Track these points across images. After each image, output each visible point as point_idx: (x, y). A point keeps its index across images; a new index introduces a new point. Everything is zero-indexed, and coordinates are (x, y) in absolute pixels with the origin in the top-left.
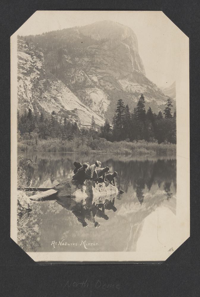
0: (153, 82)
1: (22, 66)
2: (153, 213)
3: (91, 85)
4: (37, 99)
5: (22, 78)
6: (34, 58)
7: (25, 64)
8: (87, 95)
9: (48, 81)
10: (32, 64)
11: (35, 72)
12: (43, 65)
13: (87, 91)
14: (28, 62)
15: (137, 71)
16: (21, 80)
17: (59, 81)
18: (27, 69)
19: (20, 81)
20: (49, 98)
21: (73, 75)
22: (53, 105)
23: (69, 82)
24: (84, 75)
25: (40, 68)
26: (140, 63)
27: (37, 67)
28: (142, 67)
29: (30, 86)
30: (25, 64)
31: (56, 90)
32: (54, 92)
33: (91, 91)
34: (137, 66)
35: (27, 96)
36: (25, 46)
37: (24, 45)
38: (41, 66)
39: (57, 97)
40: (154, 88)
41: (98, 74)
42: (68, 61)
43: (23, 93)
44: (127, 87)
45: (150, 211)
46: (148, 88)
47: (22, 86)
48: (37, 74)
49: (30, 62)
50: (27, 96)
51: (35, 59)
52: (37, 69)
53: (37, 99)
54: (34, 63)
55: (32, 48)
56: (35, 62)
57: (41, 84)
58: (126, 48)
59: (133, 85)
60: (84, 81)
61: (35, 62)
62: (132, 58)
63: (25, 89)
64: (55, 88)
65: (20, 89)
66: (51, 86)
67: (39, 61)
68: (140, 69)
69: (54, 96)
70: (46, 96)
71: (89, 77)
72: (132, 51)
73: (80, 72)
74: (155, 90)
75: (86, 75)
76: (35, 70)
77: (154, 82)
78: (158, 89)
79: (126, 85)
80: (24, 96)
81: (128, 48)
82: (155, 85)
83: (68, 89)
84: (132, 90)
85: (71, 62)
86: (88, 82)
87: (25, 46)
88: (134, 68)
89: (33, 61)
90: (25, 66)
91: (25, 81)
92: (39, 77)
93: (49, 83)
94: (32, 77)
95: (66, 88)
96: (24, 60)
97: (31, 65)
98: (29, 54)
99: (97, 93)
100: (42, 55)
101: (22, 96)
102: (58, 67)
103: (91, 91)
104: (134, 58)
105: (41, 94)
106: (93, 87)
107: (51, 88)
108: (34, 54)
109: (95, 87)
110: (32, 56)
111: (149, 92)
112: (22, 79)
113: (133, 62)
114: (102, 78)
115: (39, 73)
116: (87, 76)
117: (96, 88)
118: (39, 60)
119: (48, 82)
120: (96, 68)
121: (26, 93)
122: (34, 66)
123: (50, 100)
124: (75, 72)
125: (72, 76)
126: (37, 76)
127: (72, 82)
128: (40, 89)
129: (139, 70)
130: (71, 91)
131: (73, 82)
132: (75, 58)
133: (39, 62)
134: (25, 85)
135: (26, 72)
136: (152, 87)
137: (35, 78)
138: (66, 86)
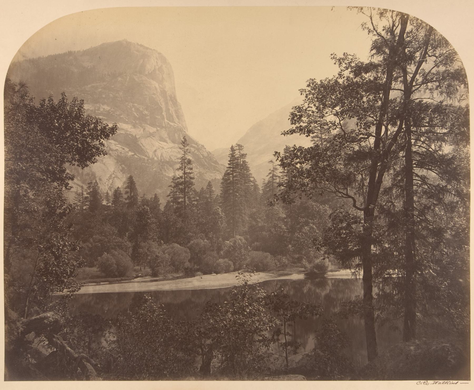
15: (172, 124)
26: (177, 112)
34: (172, 116)
40: (201, 151)
58: (153, 86)
59: (165, 147)
62: (163, 104)
68: (176, 120)
72: (164, 93)
74: (202, 155)
78: (207, 153)
79: (155, 148)
81: (155, 87)
84: (164, 155)
99: (104, 162)
104: (167, 104)
113: (164, 109)
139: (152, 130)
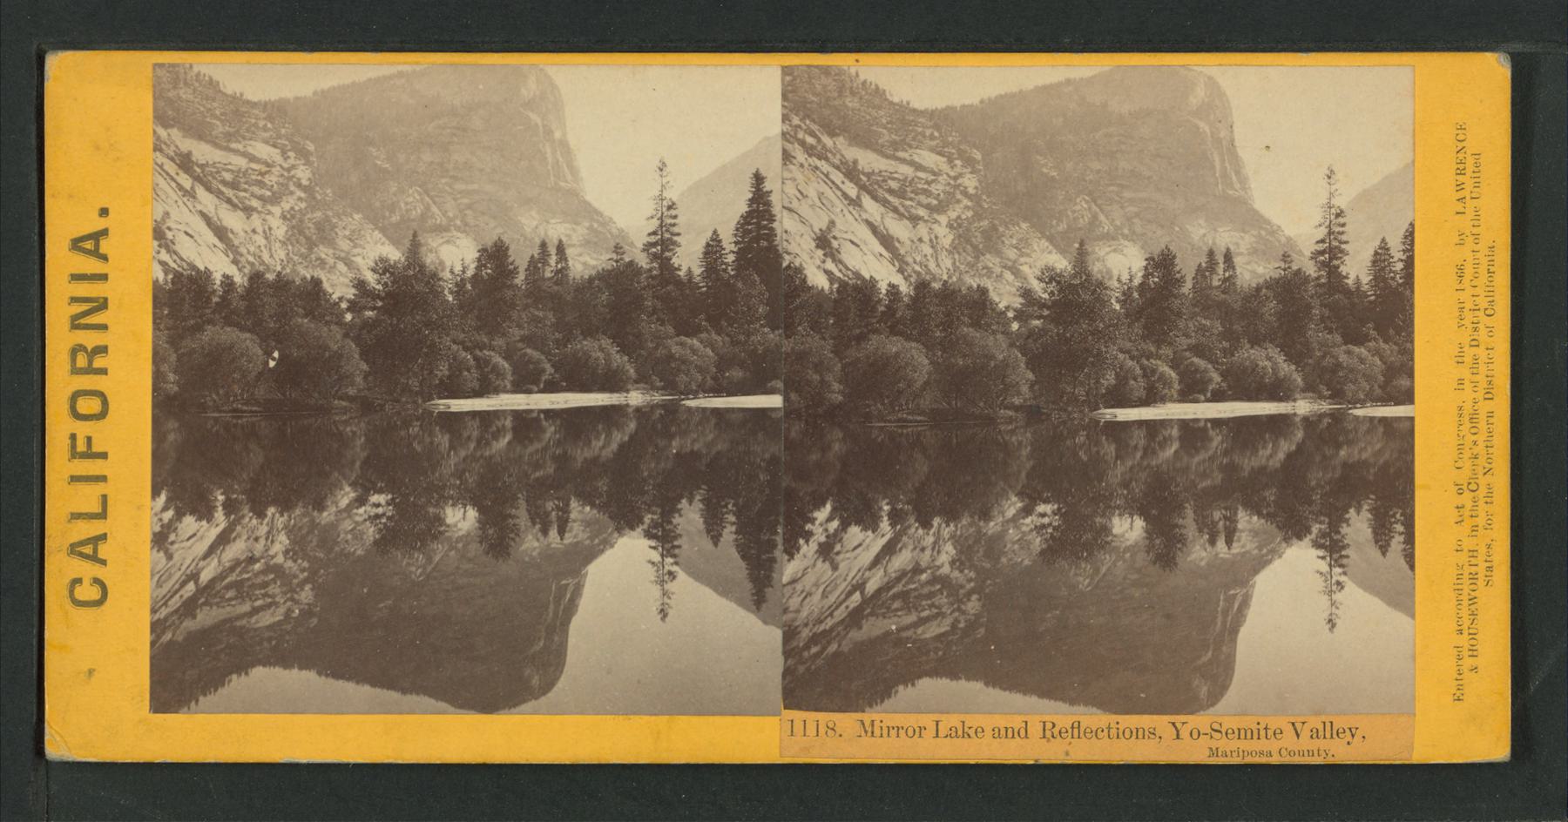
0: (606, 214)
1: (259, 178)
2: (609, 553)
3: (440, 225)
4: (301, 263)
5: (260, 209)
6: (289, 157)
7: (266, 173)
8: (431, 251)
9: (327, 216)
10: (286, 174)
11: (292, 193)
12: (314, 174)
13: (430, 240)
14: (273, 170)
16: (255, 216)
17: (356, 217)
18: (272, 186)
19: (252, 218)
20: (331, 261)
22: (342, 279)
23: (384, 218)
24: (422, 200)
25: (305, 182)
27: (299, 179)
28: (574, 171)
29: (280, 230)
30: (266, 173)
31: (350, 239)
32: (344, 245)
33: (441, 241)
35: (271, 256)
36: (266, 125)
37: (261, 124)
38: (309, 179)
39: (353, 259)
41: (459, 196)
42: (379, 163)
43: (263, 248)
44: (536, 227)
45: (602, 547)
46: (590, 228)
47: (259, 230)
48: (300, 199)
49: (278, 168)
50: (271, 256)
51: (292, 161)
52: (299, 185)
53: (301, 263)
54: (289, 170)
55: (283, 131)
56: (293, 167)
57: (310, 225)
60: (422, 215)
61: (293, 167)
63: (266, 238)
64: (347, 233)
65: (256, 237)
66: (337, 230)
67: (304, 165)
69: (343, 255)
70: (323, 256)
71: (435, 203)
73: (411, 191)
75: (427, 199)
76: (292, 188)
77: (607, 213)
80: (266, 257)
82: (611, 218)
83: (380, 235)
84: (550, 233)
85: (387, 166)
86: (432, 217)
87: (266, 125)
88: (554, 176)
89: (286, 165)
90: (266, 179)
91: (268, 217)
92: (303, 205)
93: (330, 221)
94: (287, 207)
95: (376, 232)
96: (263, 163)
97: (282, 175)
98: (274, 146)
100: (311, 147)
101: (260, 257)
102: (354, 179)
105: (310, 249)
106: (446, 229)
107: (337, 234)
108: (289, 147)
109: (452, 228)
110: (284, 153)
111: (595, 240)
112: (259, 212)
113: (550, 160)
114: (469, 207)
115: (303, 195)
116: (430, 202)
117: (455, 233)
118: (303, 162)
119: (327, 219)
120: (455, 178)
121: (270, 249)
122: (290, 178)
123: (334, 267)
125: (390, 202)
126: (299, 203)
127: (391, 217)
128: (308, 239)
129: (566, 182)
130: (387, 242)
133: (302, 167)
134: (266, 227)
135: (268, 193)
136: (603, 224)
137: (292, 208)
138: (377, 228)
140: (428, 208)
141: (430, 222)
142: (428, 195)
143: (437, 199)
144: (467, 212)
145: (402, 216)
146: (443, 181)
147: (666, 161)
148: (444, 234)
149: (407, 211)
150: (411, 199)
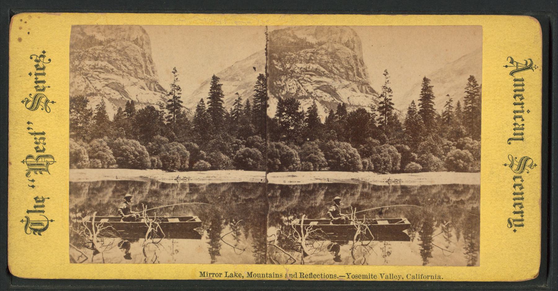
3: (305, 96)
21: (284, 84)
24: (297, 84)
33: (305, 103)
59: (356, 96)
75: (299, 84)
103: (305, 103)
124: (286, 80)
127: (282, 92)
131: (284, 93)
132: (287, 64)
138: (275, 96)
139: (346, 82)
140: (299, 88)
141: (301, 94)
142: (300, 83)
143: (303, 84)
144: (318, 90)
145: (287, 92)
146: (307, 76)
147: (388, 71)
148: (307, 100)
149: (290, 89)
150: (291, 84)
